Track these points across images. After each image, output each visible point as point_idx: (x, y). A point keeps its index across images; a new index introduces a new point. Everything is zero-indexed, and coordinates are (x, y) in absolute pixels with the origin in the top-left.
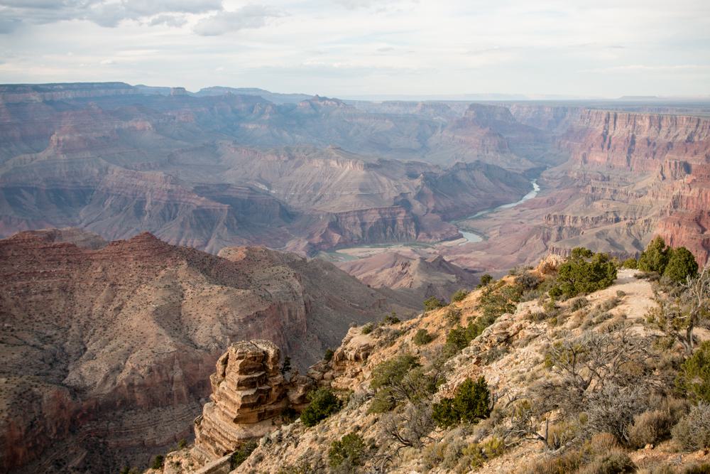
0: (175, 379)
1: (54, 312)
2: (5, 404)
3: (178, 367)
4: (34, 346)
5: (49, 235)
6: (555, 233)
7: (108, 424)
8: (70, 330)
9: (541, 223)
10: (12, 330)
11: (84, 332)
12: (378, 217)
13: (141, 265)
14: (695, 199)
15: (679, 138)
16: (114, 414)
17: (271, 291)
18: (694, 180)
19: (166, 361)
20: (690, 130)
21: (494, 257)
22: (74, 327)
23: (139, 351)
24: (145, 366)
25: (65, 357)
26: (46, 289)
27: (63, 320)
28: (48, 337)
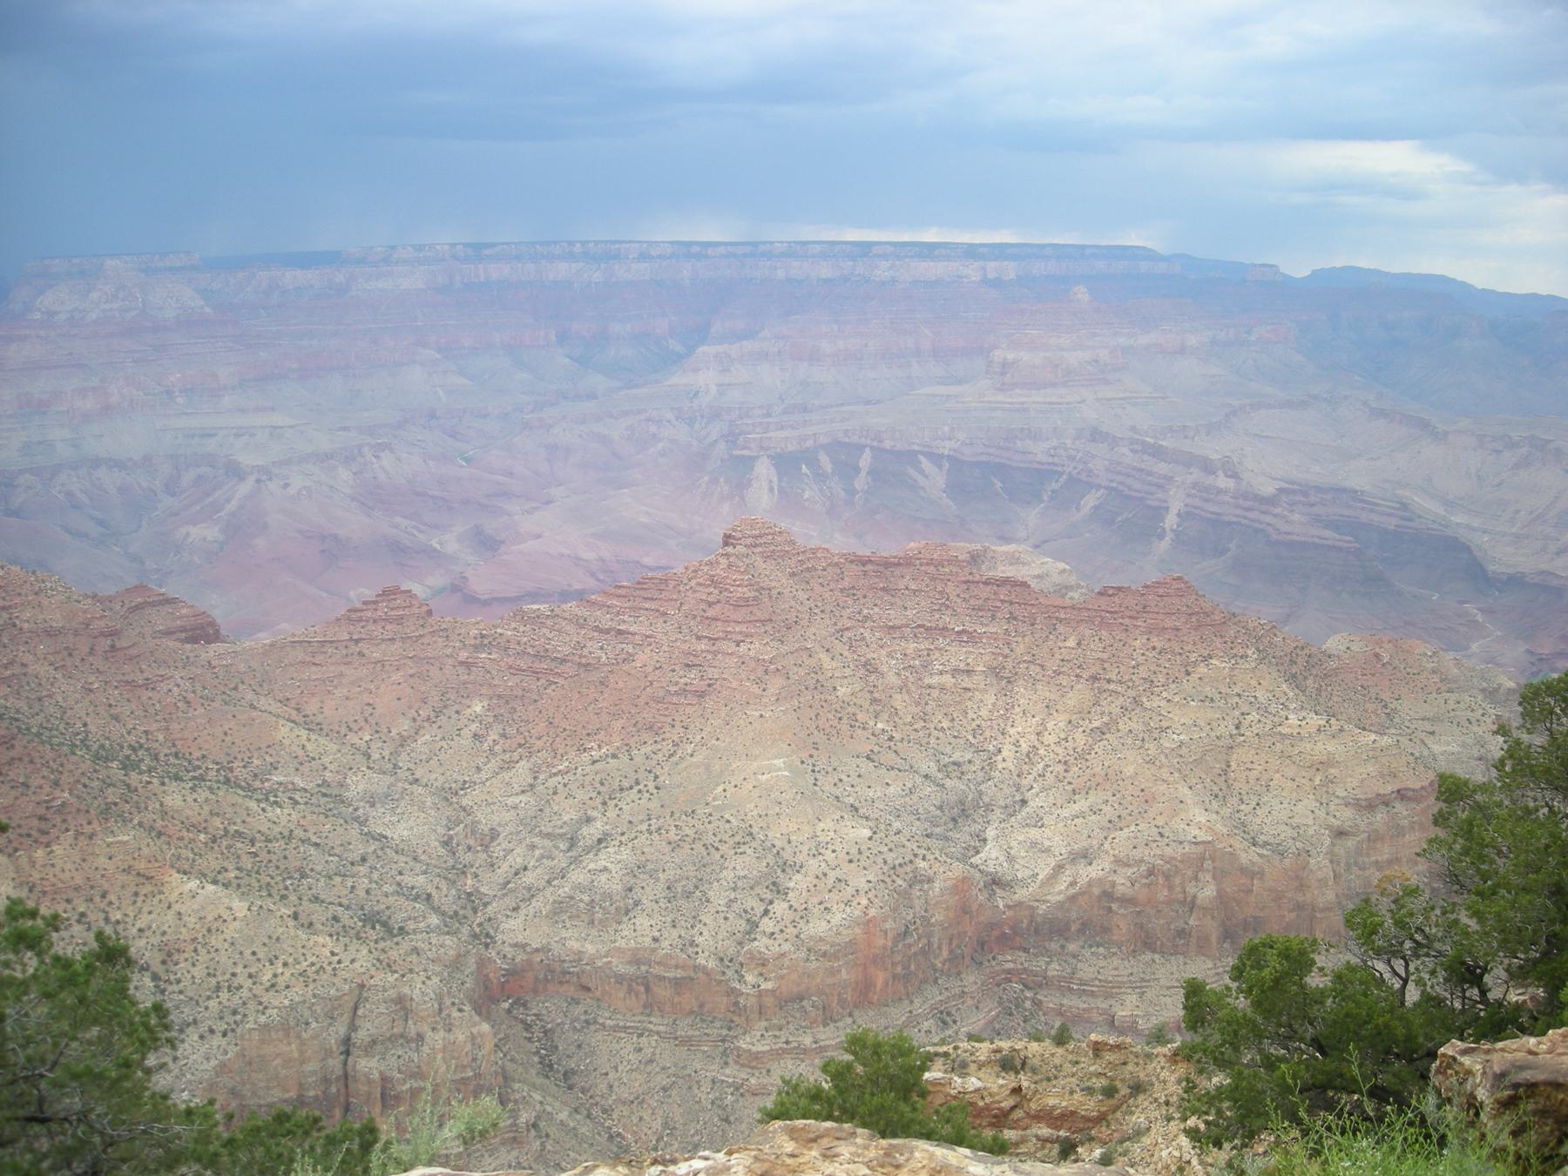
0: (1198, 902)
1: (971, 715)
2: (864, 880)
3: (1208, 877)
4: (926, 776)
5: (972, 557)
7: (1048, 963)
8: (999, 758)
10: (891, 739)
11: (1026, 767)
13: (1159, 645)
16: (1063, 947)
17: (1436, 748)
19: (1186, 859)
22: (1005, 753)
23: (1133, 828)
24: (1142, 861)
25: (981, 811)
26: (962, 666)
27: (988, 734)
28: (954, 763)
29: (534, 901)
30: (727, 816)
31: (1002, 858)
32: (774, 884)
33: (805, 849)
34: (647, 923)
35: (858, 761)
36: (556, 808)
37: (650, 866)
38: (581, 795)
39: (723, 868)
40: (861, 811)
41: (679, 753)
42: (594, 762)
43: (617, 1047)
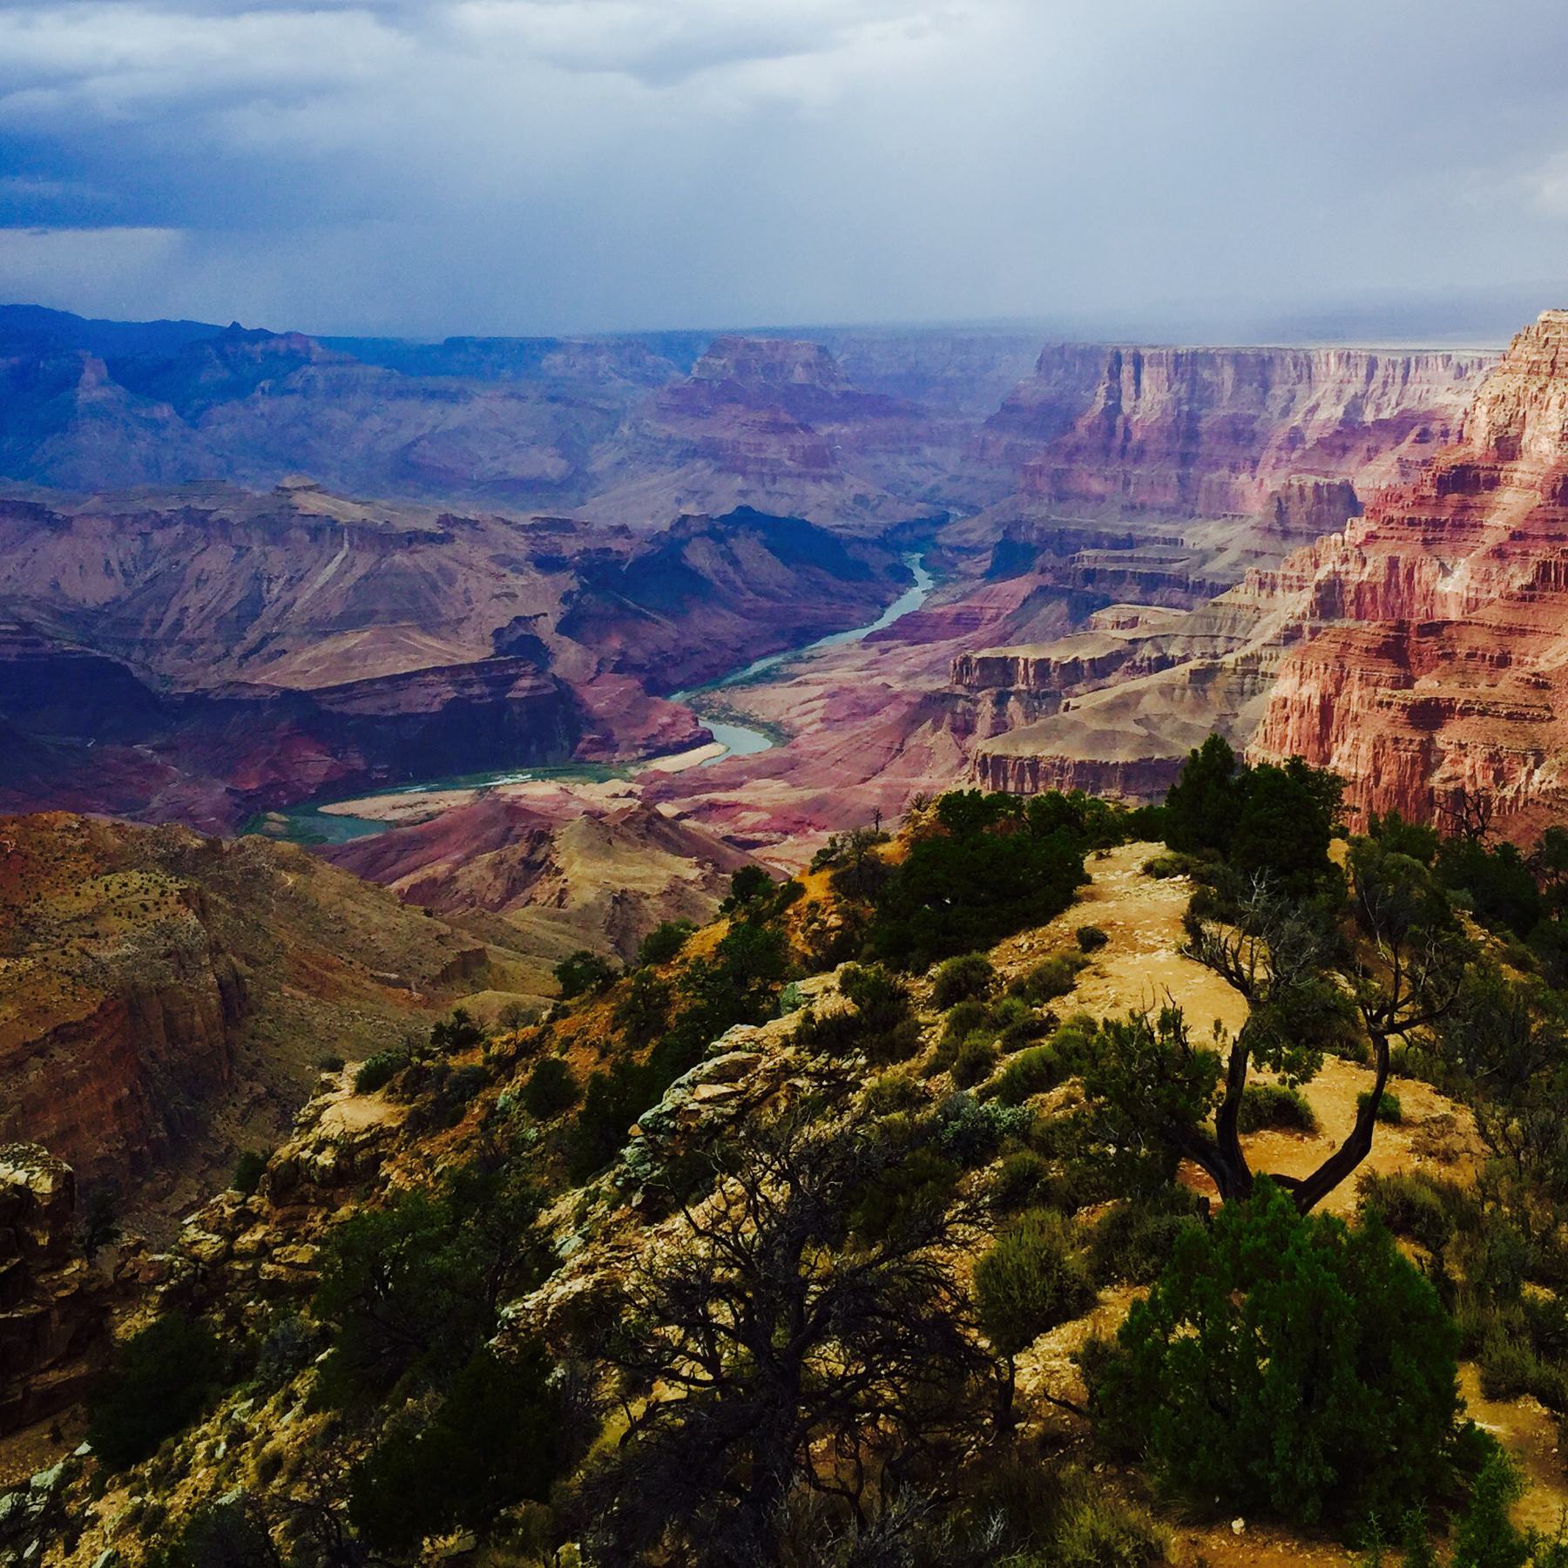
6: (986, 708)
9: (942, 684)
12: (449, 692)
14: (1380, 590)
15: (1322, 415)
18: (1371, 537)
20: (1350, 391)
21: (808, 794)
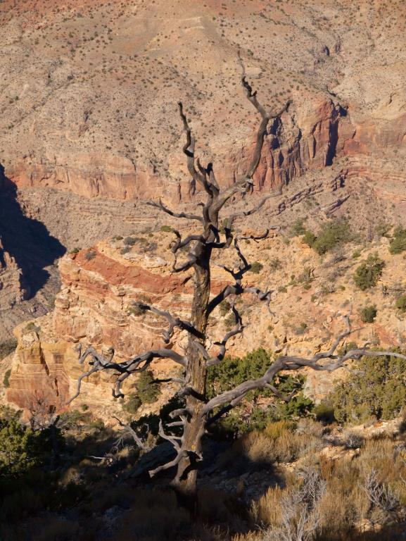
8: (358, 14)
16: (396, 152)
22: (363, 10)
29: (23, 121)
30: (159, 59)
31: (354, 88)
32: (192, 107)
33: (214, 83)
34: (102, 136)
35: (254, 17)
36: (37, 55)
37: (103, 96)
38: (55, 44)
39: (155, 97)
40: (255, 55)
41: (126, 12)
42: (65, 20)
43: (83, 222)
